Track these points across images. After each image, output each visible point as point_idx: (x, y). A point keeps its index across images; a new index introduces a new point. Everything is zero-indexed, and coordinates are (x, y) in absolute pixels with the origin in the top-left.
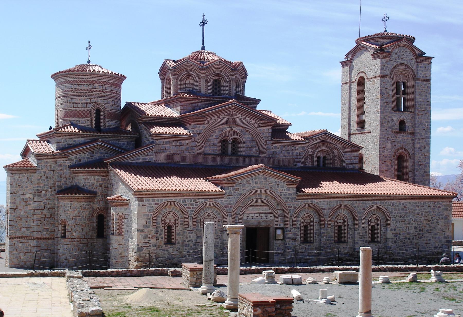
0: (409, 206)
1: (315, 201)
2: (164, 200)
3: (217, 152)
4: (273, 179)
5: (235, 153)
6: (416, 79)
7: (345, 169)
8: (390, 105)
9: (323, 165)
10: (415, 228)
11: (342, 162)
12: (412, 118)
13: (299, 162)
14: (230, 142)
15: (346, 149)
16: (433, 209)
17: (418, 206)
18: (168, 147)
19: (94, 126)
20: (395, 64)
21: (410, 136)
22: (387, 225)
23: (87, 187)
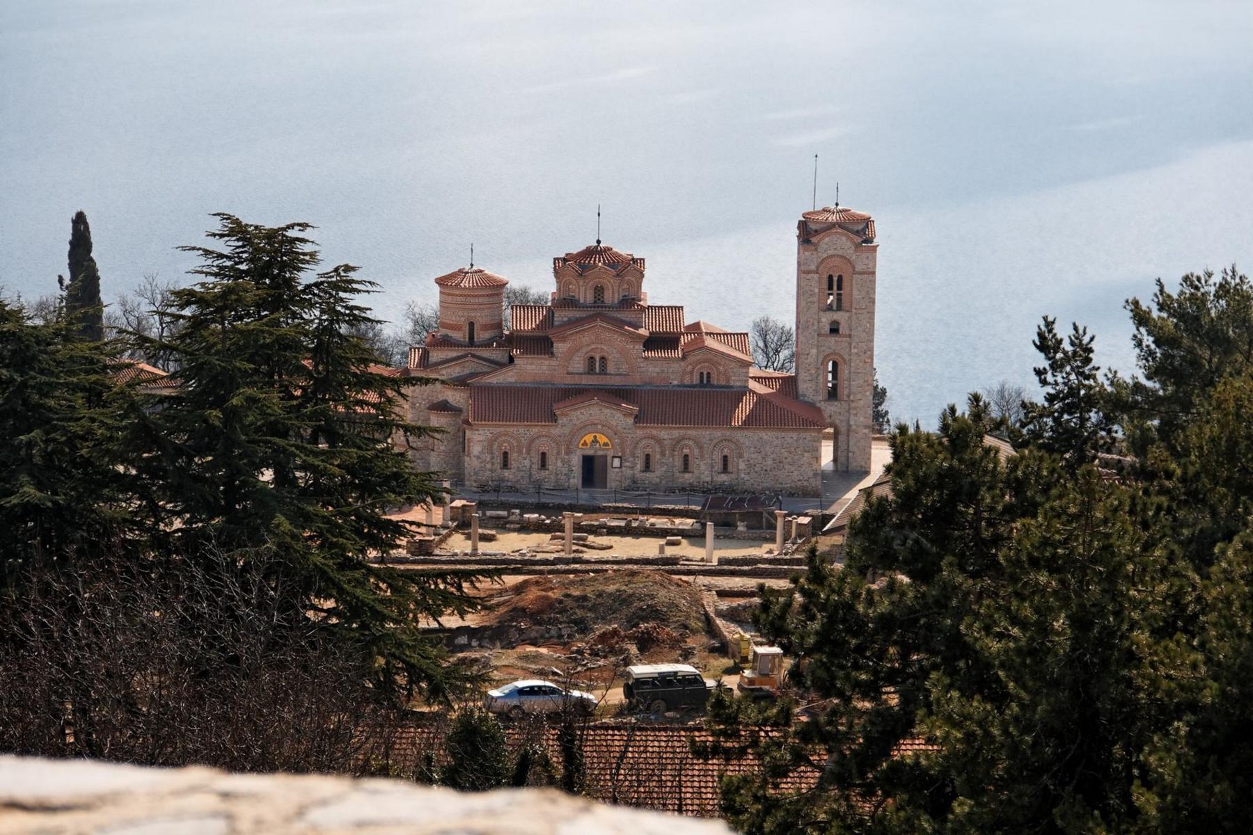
0: (765, 437)
1: (654, 432)
2: (499, 430)
3: (581, 370)
4: (607, 411)
5: (604, 371)
6: (855, 272)
7: (732, 387)
8: (816, 305)
9: (708, 381)
10: (774, 460)
11: (728, 380)
12: (850, 318)
13: (675, 379)
14: (598, 359)
15: (733, 365)
16: (797, 441)
17: (777, 438)
18: (529, 367)
19: (467, 340)
20: (825, 256)
21: (845, 339)
22: (741, 456)
23: (453, 403)
